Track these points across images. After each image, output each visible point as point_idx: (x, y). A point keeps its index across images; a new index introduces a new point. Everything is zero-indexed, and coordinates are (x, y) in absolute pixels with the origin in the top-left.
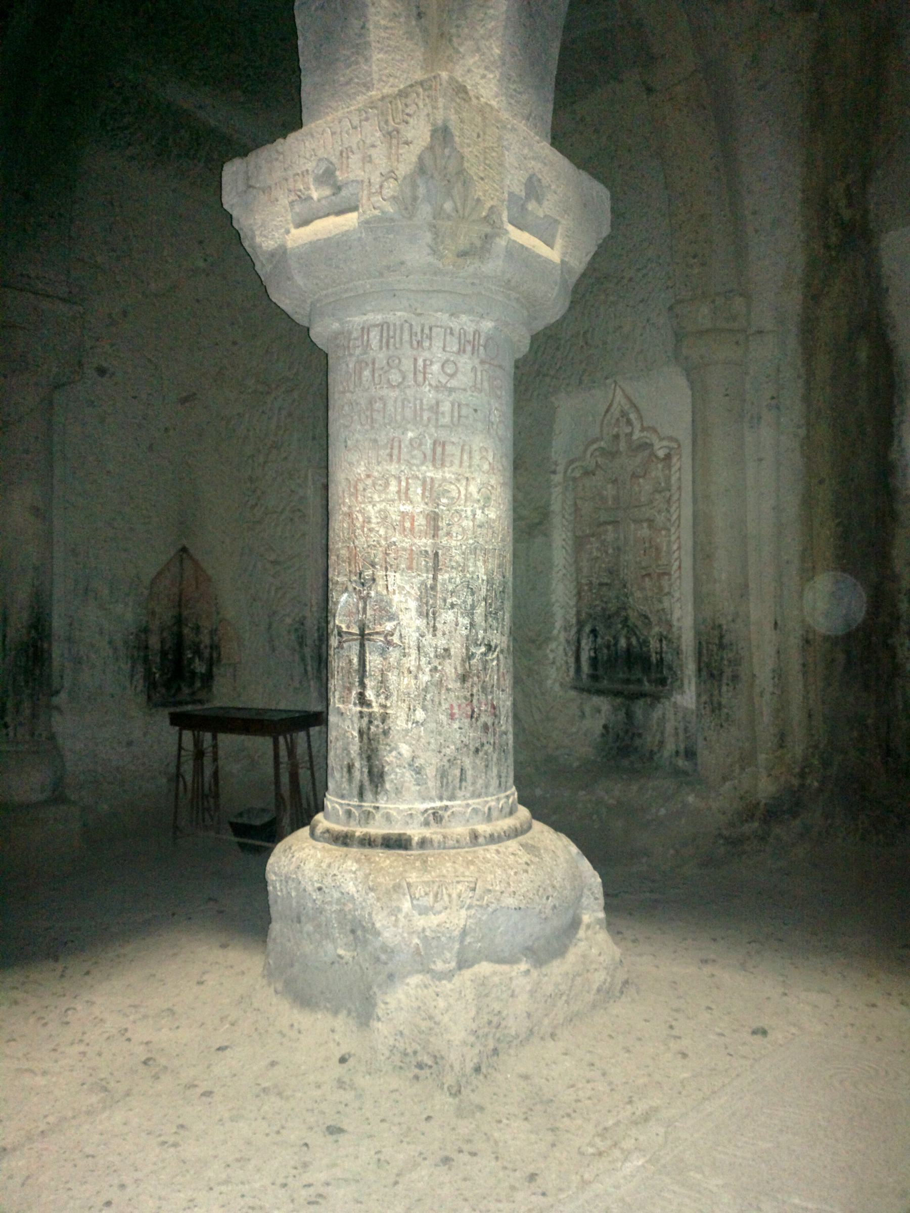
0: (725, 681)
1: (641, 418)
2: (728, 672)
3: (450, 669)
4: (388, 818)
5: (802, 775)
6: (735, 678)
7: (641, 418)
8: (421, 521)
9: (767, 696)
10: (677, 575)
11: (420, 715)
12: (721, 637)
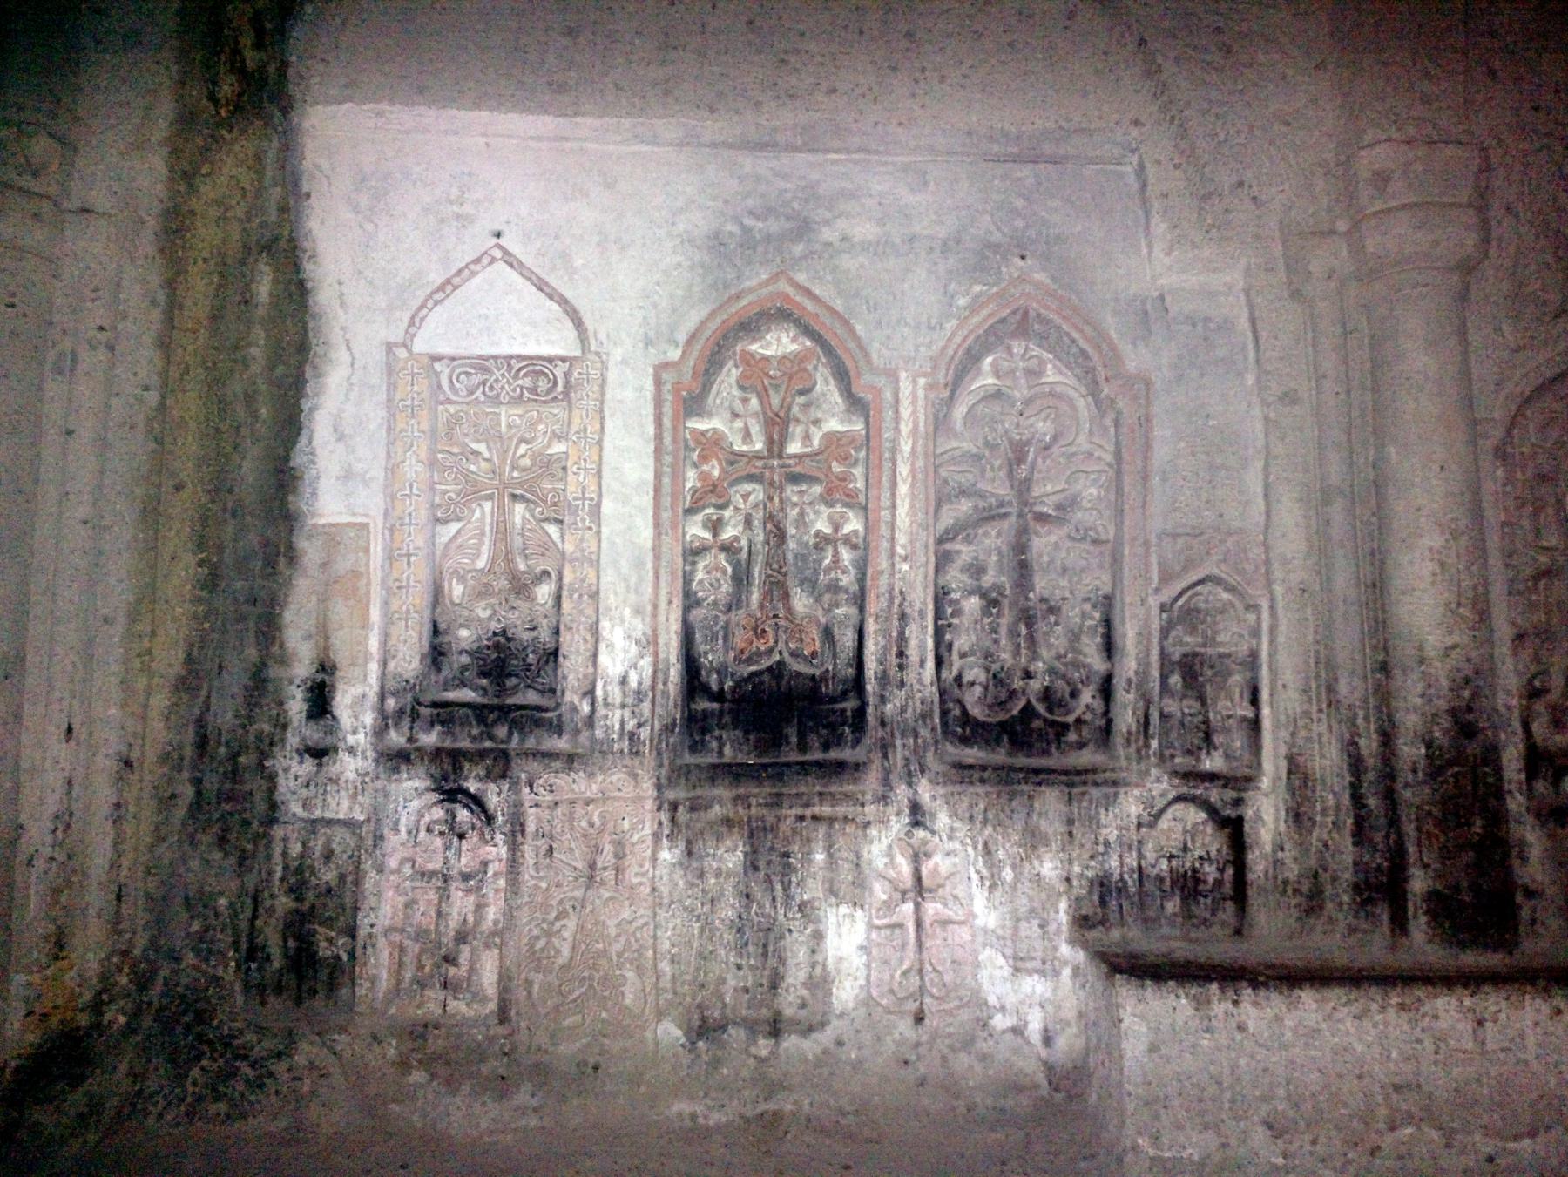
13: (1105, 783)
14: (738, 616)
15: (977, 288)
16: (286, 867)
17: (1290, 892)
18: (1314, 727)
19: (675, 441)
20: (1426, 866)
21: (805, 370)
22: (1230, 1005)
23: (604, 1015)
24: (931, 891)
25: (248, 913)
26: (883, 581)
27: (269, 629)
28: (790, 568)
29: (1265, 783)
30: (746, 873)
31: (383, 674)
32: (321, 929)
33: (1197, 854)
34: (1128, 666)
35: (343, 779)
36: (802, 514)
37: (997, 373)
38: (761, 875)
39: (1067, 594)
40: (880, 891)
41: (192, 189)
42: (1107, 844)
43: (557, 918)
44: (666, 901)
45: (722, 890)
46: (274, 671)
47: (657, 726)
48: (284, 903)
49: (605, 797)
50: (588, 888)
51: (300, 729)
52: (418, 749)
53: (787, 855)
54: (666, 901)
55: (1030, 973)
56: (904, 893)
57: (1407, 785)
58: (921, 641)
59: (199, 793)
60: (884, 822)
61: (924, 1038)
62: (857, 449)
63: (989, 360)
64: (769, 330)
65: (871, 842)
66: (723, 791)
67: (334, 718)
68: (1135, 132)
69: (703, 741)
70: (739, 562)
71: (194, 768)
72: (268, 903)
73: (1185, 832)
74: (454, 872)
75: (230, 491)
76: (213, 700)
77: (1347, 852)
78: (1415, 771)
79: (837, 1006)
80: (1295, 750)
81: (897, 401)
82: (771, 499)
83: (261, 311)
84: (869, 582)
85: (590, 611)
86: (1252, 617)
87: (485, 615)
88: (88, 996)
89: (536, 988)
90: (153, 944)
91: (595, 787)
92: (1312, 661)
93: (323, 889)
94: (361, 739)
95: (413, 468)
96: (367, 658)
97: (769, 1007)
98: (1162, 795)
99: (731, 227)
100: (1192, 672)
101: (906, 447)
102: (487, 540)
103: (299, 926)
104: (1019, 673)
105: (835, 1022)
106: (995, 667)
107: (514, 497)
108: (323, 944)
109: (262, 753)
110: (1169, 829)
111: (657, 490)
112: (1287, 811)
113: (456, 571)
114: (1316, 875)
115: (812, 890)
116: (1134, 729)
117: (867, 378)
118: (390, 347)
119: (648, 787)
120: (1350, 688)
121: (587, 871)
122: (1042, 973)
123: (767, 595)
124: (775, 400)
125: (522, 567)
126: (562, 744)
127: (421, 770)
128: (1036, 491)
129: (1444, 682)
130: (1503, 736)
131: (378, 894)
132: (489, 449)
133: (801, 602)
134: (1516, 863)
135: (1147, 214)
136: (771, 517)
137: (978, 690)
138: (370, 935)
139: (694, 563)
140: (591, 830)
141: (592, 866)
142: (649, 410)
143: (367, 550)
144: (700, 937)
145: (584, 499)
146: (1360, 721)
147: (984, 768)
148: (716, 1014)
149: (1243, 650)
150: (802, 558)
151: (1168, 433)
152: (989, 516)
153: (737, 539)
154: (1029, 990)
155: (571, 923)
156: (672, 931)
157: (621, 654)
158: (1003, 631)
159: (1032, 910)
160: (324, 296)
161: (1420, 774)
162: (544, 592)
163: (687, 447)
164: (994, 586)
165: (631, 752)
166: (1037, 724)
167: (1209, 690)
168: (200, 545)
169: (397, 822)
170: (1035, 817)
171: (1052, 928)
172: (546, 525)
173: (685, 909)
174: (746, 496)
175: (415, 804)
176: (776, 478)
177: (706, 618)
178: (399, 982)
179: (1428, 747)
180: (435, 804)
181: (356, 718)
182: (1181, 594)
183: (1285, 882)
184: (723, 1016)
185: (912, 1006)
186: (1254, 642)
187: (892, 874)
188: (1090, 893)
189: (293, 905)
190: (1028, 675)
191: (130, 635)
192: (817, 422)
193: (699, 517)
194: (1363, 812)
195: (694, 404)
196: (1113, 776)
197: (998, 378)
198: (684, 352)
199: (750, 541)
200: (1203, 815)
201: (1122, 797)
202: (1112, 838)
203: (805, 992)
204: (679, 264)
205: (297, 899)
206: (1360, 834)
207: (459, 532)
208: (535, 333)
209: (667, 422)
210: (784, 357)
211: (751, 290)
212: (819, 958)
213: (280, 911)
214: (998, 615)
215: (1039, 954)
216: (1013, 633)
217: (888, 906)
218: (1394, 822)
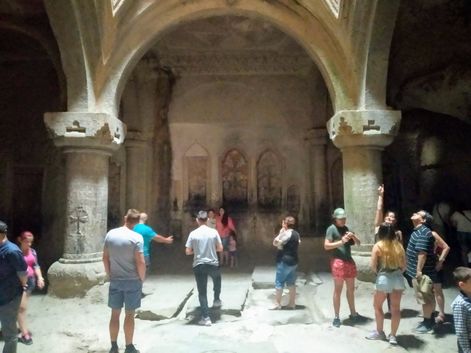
3: (99, 225)
4: (85, 257)
8: (93, 195)
11: (92, 235)
34: (283, 197)
58: (255, 194)
95: (186, 172)
133: (239, 188)
162: (204, 188)
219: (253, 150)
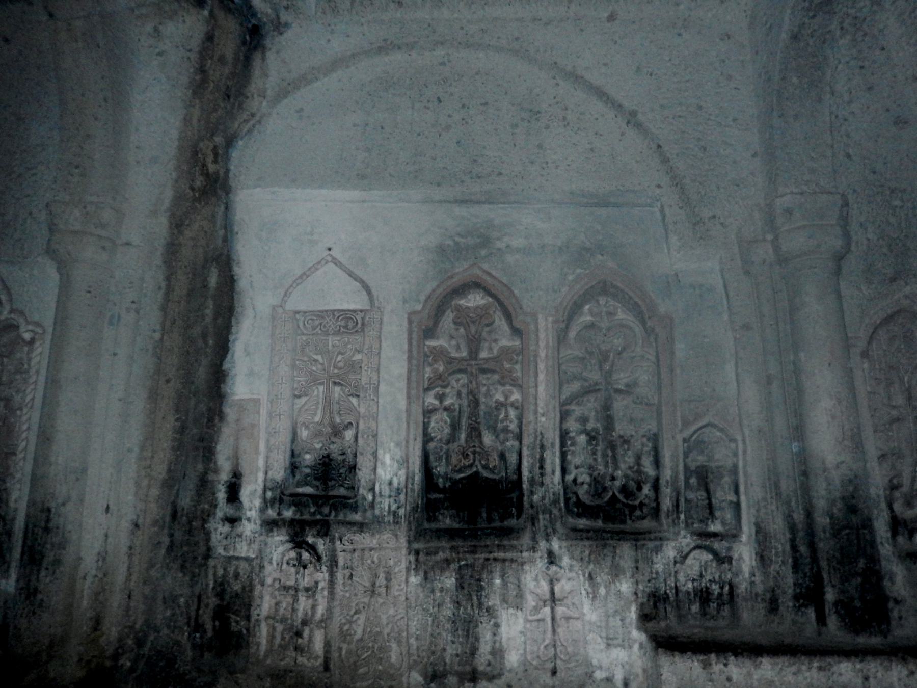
0: (44, 565)
1: (11, 300)
2: (50, 556)
5: (116, 656)
6: (57, 562)
7: (11, 300)
9: (89, 579)
10: (22, 455)
12: (48, 520)
13: (656, 539)
14: (454, 446)
15: (578, 271)
16: (215, 582)
17: (759, 600)
18: (769, 506)
19: (418, 352)
20: (833, 586)
21: (488, 314)
22: (722, 666)
23: (380, 667)
24: (559, 600)
25: (195, 607)
26: (531, 427)
27: (208, 453)
28: (481, 420)
29: (744, 538)
30: (457, 590)
31: (266, 480)
32: (233, 616)
33: (708, 578)
34: (667, 474)
35: (244, 537)
36: (488, 390)
37: (591, 313)
38: (466, 591)
39: (633, 433)
40: (531, 601)
41: (181, 233)
42: (657, 573)
43: (355, 613)
44: (413, 605)
45: (444, 599)
46: (211, 477)
47: (408, 508)
48: (213, 601)
49: (380, 548)
50: (371, 597)
51: (223, 509)
52: (283, 520)
53: (479, 580)
54: (413, 605)
55: (616, 646)
56: (545, 602)
57: (820, 540)
58: (553, 460)
59: (172, 541)
60: (532, 561)
61: (557, 683)
62: (517, 355)
63: (587, 307)
64: (470, 293)
65: (526, 573)
66: (444, 544)
67: (241, 502)
68: (658, 191)
69: (434, 515)
70: (454, 417)
71: (170, 528)
72: (206, 601)
73: (701, 566)
74: (301, 587)
75: (193, 383)
76: (181, 492)
77: (789, 579)
78: (825, 532)
79: (508, 665)
80: (759, 520)
81: (537, 330)
82: (471, 382)
83: (212, 291)
84: (524, 428)
85: (373, 445)
86: (733, 445)
87: (318, 446)
88: (110, 651)
89: (344, 652)
90: (147, 622)
91: (375, 541)
92: (766, 470)
93: (234, 594)
94: (253, 514)
95: (284, 370)
96: (257, 470)
97: (471, 665)
98: (687, 546)
99: (447, 242)
100: (704, 478)
101: (542, 354)
102: (320, 407)
103: (222, 613)
104: (608, 478)
105: (507, 674)
106: (595, 474)
107: (335, 383)
108: (234, 624)
109: (204, 520)
110: (692, 564)
111: (409, 379)
112: (756, 554)
113: (304, 423)
114: (773, 591)
115: (494, 601)
116: (671, 508)
117: (521, 318)
118: (274, 308)
119: (403, 541)
120: (787, 486)
121: (371, 588)
122: (623, 646)
123: (469, 436)
124: (473, 329)
125: (338, 420)
126: (357, 517)
127: (284, 531)
128: (615, 376)
129: (837, 482)
130: (876, 512)
131: (261, 598)
132: (323, 358)
133: (488, 439)
134: (886, 583)
135: (667, 233)
136: (470, 392)
137: (586, 487)
138: (257, 620)
139: (429, 418)
140: (373, 565)
141: (373, 585)
142: (406, 336)
143: (258, 413)
144: (432, 625)
145: (370, 384)
146: (793, 503)
147: (588, 531)
148: (441, 669)
149: (729, 463)
150: (488, 414)
151: (683, 346)
152: (588, 391)
153: (453, 404)
154: (615, 657)
155: (362, 618)
156: (416, 622)
157: (389, 467)
158: (599, 454)
159: (616, 611)
160: (243, 284)
161: (828, 534)
163: (426, 356)
164: (593, 429)
165: (394, 522)
166: (619, 505)
167: (712, 487)
168: (177, 411)
169: (271, 559)
170: (617, 558)
171: (628, 620)
172: (351, 398)
173: (424, 609)
174: (458, 380)
175: (281, 549)
176: (474, 371)
177: (436, 448)
178: (272, 646)
179: (831, 518)
180: (291, 549)
181: (251, 502)
182: (695, 432)
183: (757, 595)
184: (445, 669)
185: (550, 665)
186: (735, 459)
187: (538, 591)
188: (648, 600)
189: (218, 602)
190: (613, 478)
191: (141, 458)
192: (496, 341)
193: (433, 393)
194: (798, 554)
195: (429, 333)
196: (660, 535)
197: (592, 316)
198: (424, 306)
199: (460, 405)
200: (711, 557)
201: (664, 548)
202: (660, 570)
203: (489, 657)
204: (421, 261)
205: (222, 599)
206: (796, 567)
207: (306, 402)
208: (345, 297)
209: (414, 343)
210: (478, 307)
211: (458, 273)
212: (497, 638)
213: (212, 606)
214: (596, 445)
215: (621, 636)
216: (605, 455)
217: (536, 609)
218: (815, 559)
219: (543, 290)
